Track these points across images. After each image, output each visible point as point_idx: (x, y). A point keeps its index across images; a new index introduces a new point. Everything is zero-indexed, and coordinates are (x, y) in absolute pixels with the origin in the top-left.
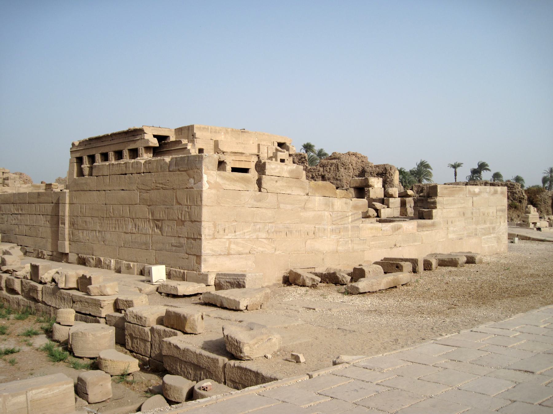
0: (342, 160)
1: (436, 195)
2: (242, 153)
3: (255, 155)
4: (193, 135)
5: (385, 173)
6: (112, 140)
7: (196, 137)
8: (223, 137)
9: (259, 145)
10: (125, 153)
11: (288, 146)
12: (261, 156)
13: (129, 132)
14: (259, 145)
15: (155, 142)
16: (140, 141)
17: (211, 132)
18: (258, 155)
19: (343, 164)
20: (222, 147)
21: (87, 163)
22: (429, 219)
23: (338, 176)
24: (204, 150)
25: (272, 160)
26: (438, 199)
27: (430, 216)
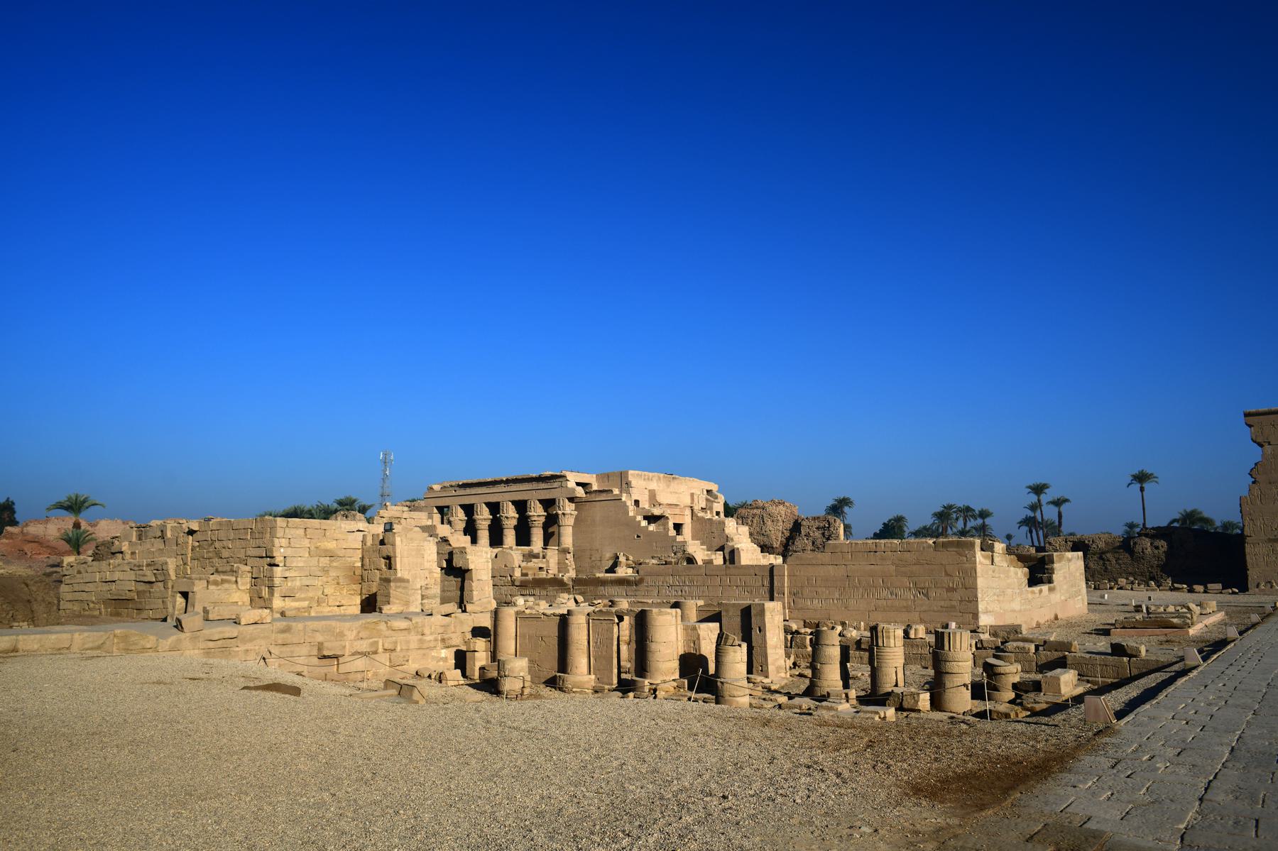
2: (677, 505)
4: (628, 484)
8: (655, 484)
14: (692, 495)
15: (580, 492)
17: (644, 479)
18: (691, 507)
20: (662, 498)
25: (706, 512)
26: (1056, 565)
27: (1050, 581)
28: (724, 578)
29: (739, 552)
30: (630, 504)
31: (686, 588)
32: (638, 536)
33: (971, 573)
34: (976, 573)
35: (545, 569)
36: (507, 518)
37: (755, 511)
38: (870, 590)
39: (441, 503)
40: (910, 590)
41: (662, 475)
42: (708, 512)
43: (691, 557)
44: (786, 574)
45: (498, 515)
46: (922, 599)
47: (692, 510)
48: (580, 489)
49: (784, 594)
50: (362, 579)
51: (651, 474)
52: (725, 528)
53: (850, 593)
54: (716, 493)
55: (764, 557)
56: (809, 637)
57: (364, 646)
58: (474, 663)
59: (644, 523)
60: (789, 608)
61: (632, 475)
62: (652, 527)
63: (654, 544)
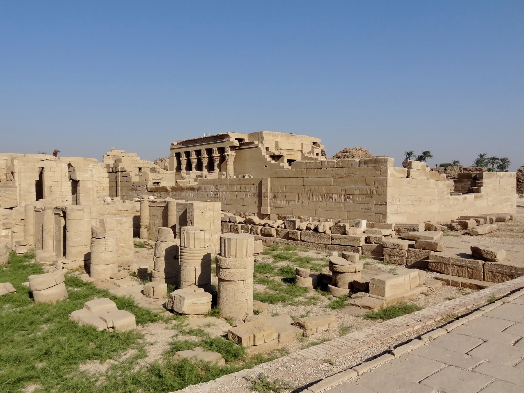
1: (482, 178)
3: (300, 151)
8: (280, 139)
9: (302, 144)
10: (215, 150)
11: (319, 145)
12: (304, 151)
14: (302, 144)
15: (237, 143)
17: (273, 136)
18: (301, 151)
20: (281, 146)
22: (478, 193)
25: (310, 154)
27: (478, 191)
28: (238, 186)
31: (220, 193)
33: (384, 183)
34: (386, 184)
36: (204, 158)
40: (342, 195)
41: (284, 134)
42: (312, 153)
47: (302, 153)
49: (267, 197)
51: (277, 133)
53: (305, 197)
54: (319, 144)
56: (260, 227)
59: (269, 159)
60: (271, 207)
61: (266, 134)
62: (273, 162)
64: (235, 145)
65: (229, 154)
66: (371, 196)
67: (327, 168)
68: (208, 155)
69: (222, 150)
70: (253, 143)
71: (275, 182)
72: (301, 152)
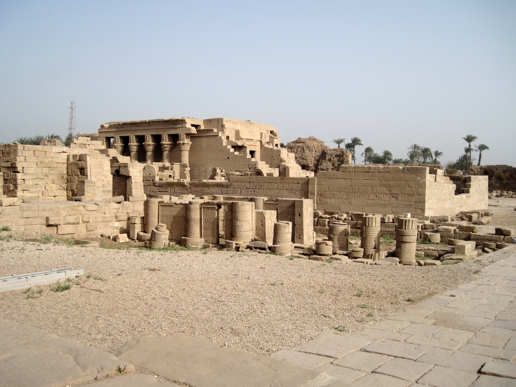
0: (307, 144)
2: (252, 140)
3: (259, 141)
4: (223, 126)
5: (343, 155)
6: (150, 125)
7: (225, 127)
8: (239, 127)
10: (164, 136)
13: (171, 121)
14: (261, 134)
15: (194, 130)
16: (181, 129)
18: (261, 141)
19: (308, 147)
20: (242, 135)
21: (120, 143)
22: (468, 193)
23: (304, 156)
24: (230, 137)
25: (270, 145)
27: (468, 192)
28: (279, 184)
29: (288, 169)
30: (224, 138)
31: (257, 190)
32: (228, 158)
33: (423, 186)
34: (425, 186)
35: (172, 176)
36: (149, 145)
37: (299, 144)
38: (364, 194)
39: (108, 135)
42: (271, 144)
43: (260, 171)
44: (316, 183)
45: (144, 143)
46: (394, 200)
47: (261, 143)
48: (193, 129)
49: (314, 195)
50: (67, 181)
52: (281, 154)
53: (353, 195)
55: (303, 172)
56: (327, 220)
57: (72, 219)
58: (135, 231)
59: (232, 150)
60: (317, 203)
62: (236, 153)
63: (238, 163)
64: (192, 132)
65: (184, 142)
66: (413, 195)
67: (374, 172)
68: (153, 142)
69: (175, 138)
70: (213, 130)
71: (322, 182)
72: (260, 143)
